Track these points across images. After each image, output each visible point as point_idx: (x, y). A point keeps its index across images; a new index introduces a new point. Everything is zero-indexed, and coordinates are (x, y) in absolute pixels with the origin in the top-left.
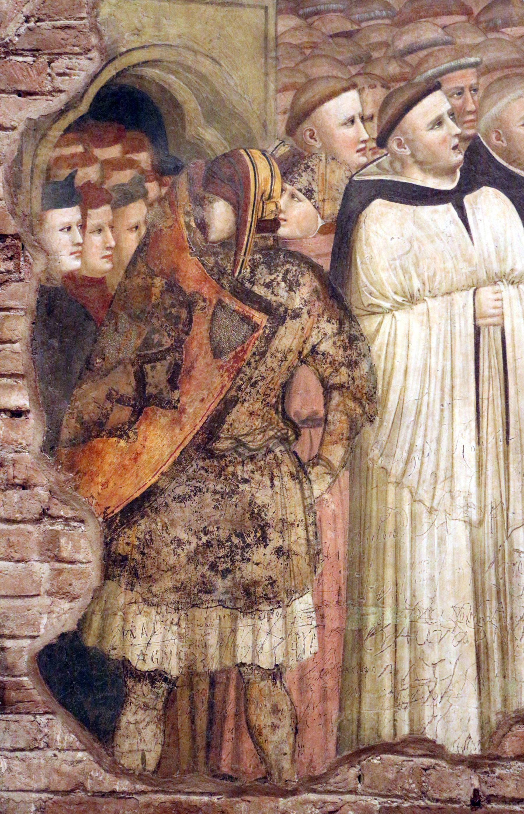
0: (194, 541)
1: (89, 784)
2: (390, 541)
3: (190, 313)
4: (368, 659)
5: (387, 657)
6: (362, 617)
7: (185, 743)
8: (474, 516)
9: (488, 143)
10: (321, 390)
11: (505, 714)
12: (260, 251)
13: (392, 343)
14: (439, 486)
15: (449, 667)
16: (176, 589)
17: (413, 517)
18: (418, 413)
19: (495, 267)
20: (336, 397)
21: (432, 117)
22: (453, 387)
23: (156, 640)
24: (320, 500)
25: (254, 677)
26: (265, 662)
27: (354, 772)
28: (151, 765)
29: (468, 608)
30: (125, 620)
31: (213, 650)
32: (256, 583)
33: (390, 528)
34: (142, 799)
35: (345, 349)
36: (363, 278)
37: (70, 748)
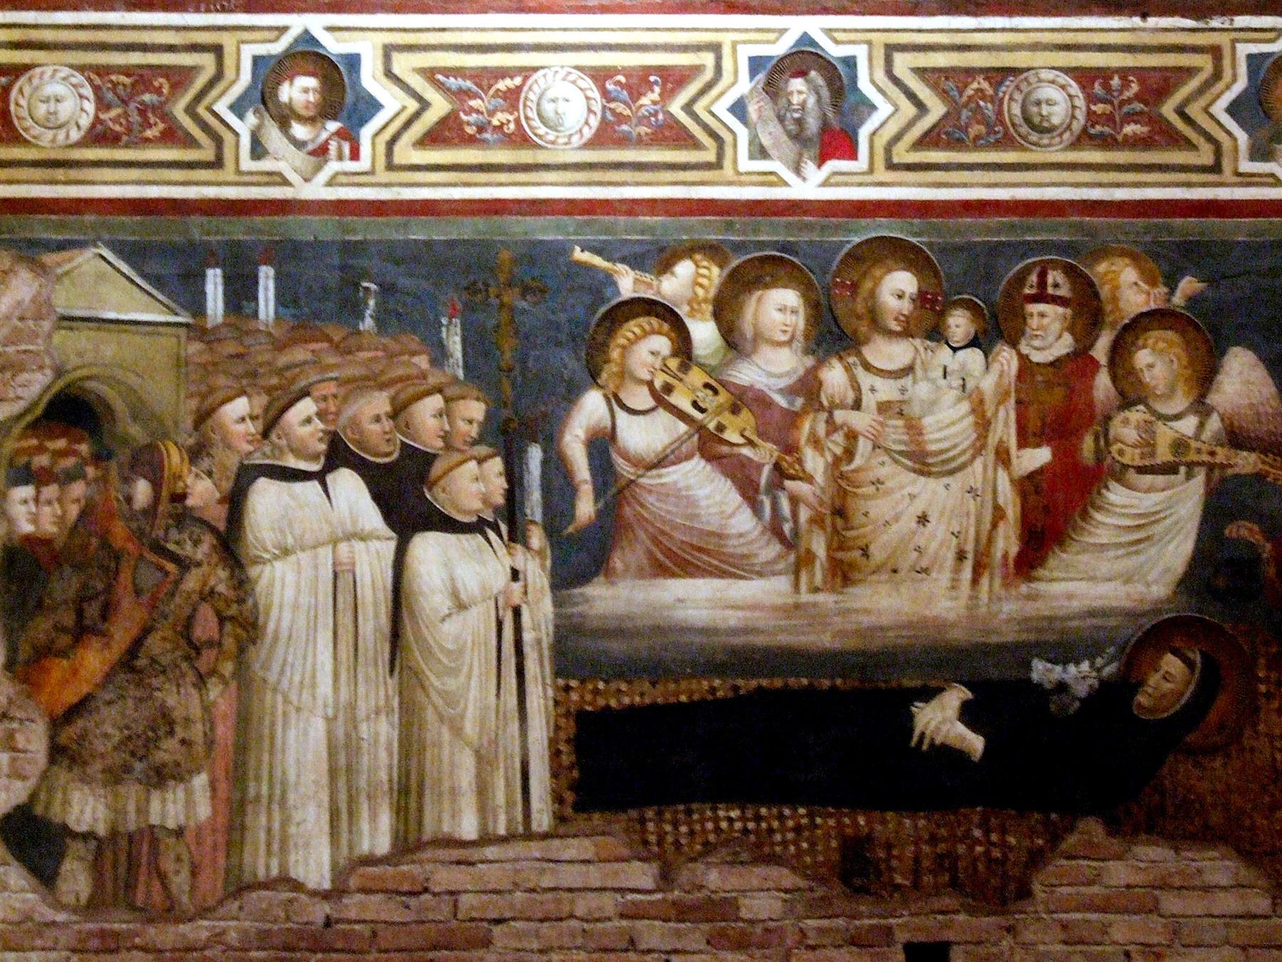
0: (118, 733)
1: (37, 917)
2: (266, 732)
3: (117, 564)
4: (249, 820)
5: (263, 820)
6: (244, 791)
7: (109, 885)
8: (330, 712)
9: (345, 434)
10: (216, 619)
11: (350, 859)
12: (171, 516)
13: (271, 584)
14: (305, 691)
15: (309, 826)
16: (103, 771)
17: (285, 714)
18: (290, 637)
19: (349, 528)
20: (228, 627)
21: (303, 416)
22: (316, 617)
23: (88, 809)
24: (214, 704)
25: (161, 835)
26: (171, 824)
27: (237, 904)
28: (83, 900)
29: (325, 780)
30: (64, 794)
31: (132, 815)
32: (164, 765)
33: (267, 722)
34: (76, 927)
35: (235, 589)
36: (250, 537)
37: (23, 890)
